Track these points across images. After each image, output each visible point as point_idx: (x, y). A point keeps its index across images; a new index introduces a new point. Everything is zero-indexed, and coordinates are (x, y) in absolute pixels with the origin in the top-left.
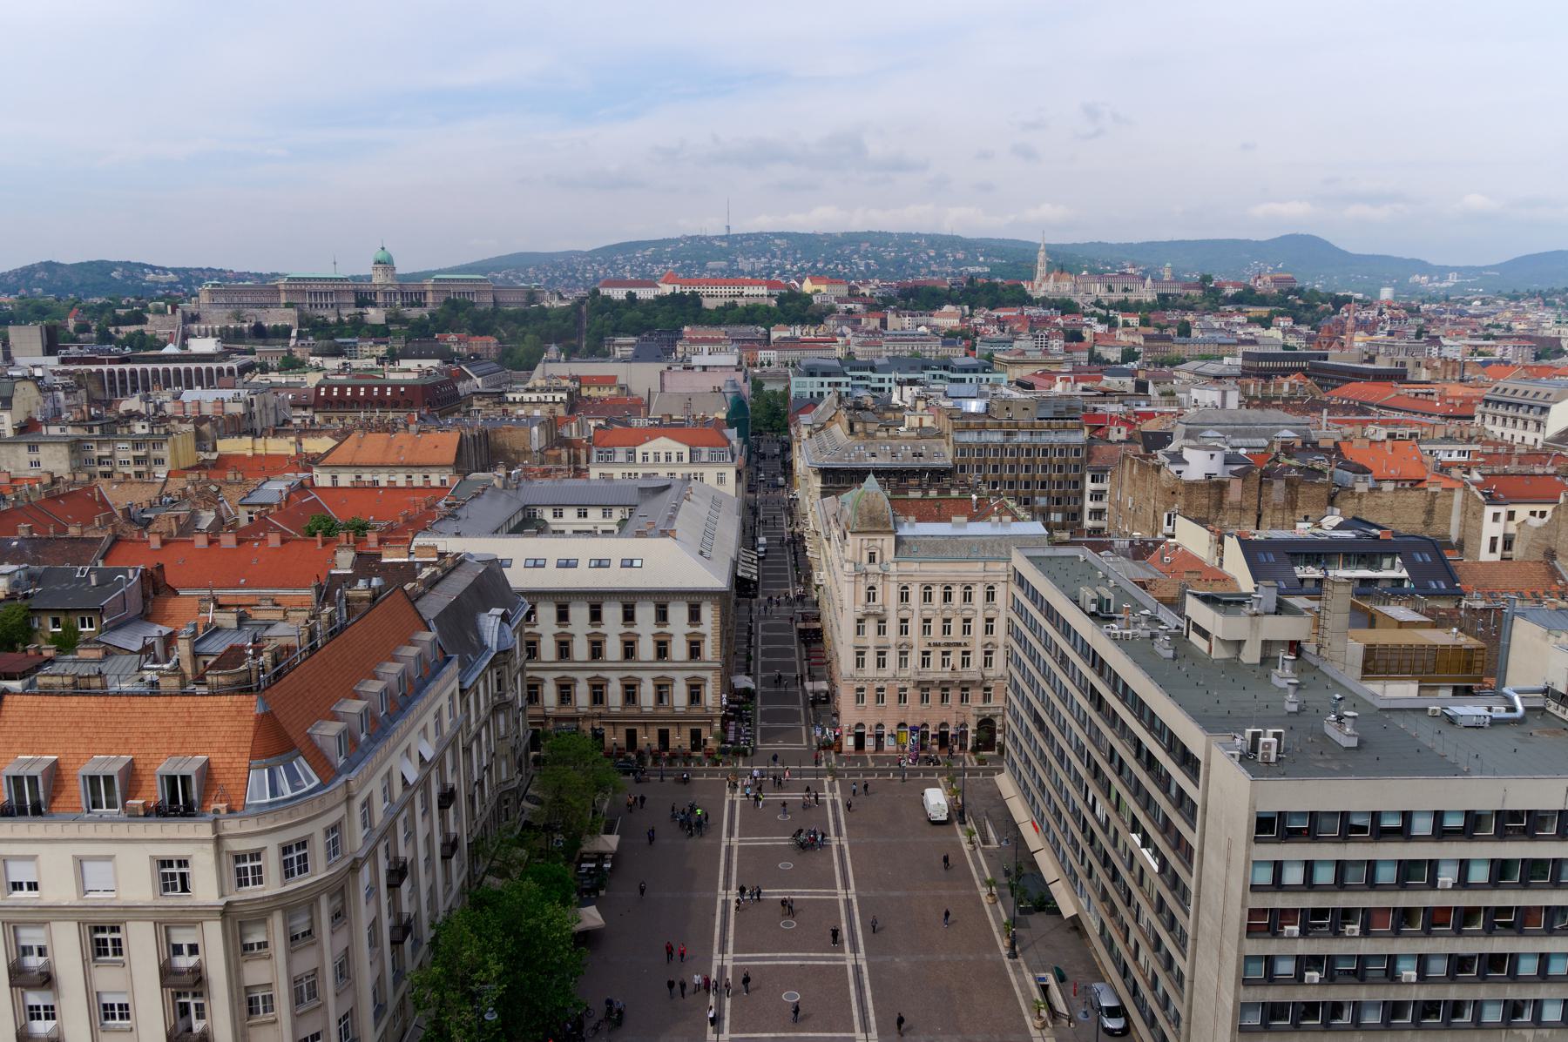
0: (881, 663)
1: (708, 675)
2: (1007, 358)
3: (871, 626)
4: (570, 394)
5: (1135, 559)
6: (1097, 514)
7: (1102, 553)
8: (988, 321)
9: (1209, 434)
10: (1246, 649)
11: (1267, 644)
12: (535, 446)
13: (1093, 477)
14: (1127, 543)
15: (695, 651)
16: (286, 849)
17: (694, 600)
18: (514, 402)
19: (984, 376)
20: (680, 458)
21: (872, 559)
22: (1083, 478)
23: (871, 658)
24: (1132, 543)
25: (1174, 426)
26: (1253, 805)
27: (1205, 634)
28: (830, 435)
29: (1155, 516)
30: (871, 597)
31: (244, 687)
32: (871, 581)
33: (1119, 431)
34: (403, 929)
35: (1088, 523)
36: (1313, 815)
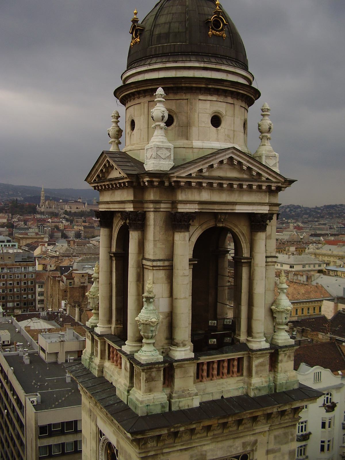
2: (21, 236)
5: (49, 320)
6: (41, 301)
7: (32, 319)
8: (19, 220)
9: (87, 266)
10: (59, 355)
11: (67, 353)
13: (39, 286)
14: (46, 313)
19: (8, 244)
22: (35, 287)
24: (48, 313)
25: (73, 264)
26: (36, 423)
27: (44, 351)
29: (59, 302)
33: (51, 267)
35: (38, 306)
36: (63, 423)
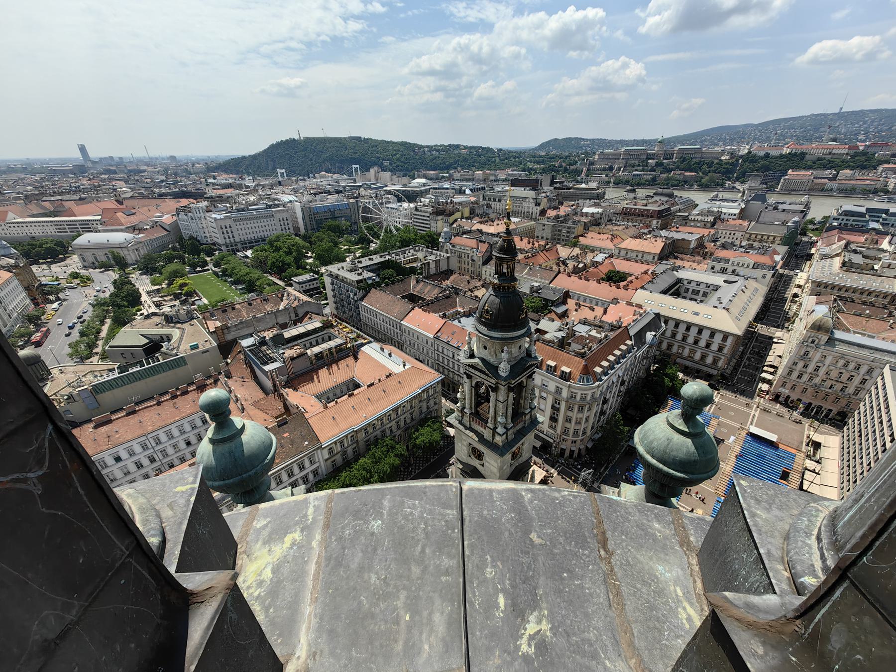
0: (800, 377)
1: (723, 358)
3: (801, 364)
4: (715, 219)
12: (692, 246)
15: (720, 349)
16: (582, 394)
17: (726, 336)
18: (691, 220)
20: (748, 266)
21: (813, 342)
23: (795, 375)
28: (831, 266)
30: (806, 353)
31: (583, 355)
32: (809, 349)
34: (602, 413)
